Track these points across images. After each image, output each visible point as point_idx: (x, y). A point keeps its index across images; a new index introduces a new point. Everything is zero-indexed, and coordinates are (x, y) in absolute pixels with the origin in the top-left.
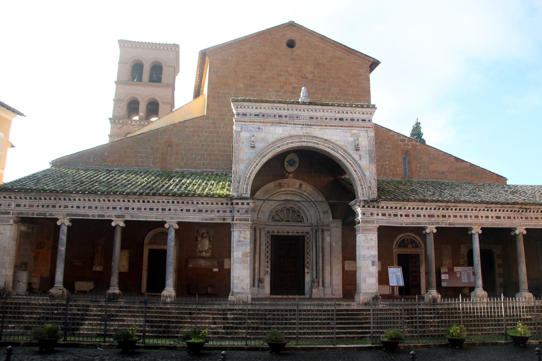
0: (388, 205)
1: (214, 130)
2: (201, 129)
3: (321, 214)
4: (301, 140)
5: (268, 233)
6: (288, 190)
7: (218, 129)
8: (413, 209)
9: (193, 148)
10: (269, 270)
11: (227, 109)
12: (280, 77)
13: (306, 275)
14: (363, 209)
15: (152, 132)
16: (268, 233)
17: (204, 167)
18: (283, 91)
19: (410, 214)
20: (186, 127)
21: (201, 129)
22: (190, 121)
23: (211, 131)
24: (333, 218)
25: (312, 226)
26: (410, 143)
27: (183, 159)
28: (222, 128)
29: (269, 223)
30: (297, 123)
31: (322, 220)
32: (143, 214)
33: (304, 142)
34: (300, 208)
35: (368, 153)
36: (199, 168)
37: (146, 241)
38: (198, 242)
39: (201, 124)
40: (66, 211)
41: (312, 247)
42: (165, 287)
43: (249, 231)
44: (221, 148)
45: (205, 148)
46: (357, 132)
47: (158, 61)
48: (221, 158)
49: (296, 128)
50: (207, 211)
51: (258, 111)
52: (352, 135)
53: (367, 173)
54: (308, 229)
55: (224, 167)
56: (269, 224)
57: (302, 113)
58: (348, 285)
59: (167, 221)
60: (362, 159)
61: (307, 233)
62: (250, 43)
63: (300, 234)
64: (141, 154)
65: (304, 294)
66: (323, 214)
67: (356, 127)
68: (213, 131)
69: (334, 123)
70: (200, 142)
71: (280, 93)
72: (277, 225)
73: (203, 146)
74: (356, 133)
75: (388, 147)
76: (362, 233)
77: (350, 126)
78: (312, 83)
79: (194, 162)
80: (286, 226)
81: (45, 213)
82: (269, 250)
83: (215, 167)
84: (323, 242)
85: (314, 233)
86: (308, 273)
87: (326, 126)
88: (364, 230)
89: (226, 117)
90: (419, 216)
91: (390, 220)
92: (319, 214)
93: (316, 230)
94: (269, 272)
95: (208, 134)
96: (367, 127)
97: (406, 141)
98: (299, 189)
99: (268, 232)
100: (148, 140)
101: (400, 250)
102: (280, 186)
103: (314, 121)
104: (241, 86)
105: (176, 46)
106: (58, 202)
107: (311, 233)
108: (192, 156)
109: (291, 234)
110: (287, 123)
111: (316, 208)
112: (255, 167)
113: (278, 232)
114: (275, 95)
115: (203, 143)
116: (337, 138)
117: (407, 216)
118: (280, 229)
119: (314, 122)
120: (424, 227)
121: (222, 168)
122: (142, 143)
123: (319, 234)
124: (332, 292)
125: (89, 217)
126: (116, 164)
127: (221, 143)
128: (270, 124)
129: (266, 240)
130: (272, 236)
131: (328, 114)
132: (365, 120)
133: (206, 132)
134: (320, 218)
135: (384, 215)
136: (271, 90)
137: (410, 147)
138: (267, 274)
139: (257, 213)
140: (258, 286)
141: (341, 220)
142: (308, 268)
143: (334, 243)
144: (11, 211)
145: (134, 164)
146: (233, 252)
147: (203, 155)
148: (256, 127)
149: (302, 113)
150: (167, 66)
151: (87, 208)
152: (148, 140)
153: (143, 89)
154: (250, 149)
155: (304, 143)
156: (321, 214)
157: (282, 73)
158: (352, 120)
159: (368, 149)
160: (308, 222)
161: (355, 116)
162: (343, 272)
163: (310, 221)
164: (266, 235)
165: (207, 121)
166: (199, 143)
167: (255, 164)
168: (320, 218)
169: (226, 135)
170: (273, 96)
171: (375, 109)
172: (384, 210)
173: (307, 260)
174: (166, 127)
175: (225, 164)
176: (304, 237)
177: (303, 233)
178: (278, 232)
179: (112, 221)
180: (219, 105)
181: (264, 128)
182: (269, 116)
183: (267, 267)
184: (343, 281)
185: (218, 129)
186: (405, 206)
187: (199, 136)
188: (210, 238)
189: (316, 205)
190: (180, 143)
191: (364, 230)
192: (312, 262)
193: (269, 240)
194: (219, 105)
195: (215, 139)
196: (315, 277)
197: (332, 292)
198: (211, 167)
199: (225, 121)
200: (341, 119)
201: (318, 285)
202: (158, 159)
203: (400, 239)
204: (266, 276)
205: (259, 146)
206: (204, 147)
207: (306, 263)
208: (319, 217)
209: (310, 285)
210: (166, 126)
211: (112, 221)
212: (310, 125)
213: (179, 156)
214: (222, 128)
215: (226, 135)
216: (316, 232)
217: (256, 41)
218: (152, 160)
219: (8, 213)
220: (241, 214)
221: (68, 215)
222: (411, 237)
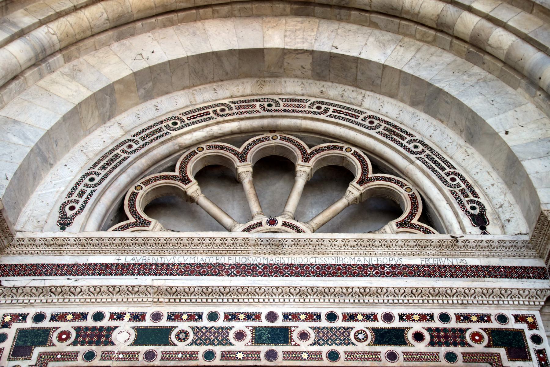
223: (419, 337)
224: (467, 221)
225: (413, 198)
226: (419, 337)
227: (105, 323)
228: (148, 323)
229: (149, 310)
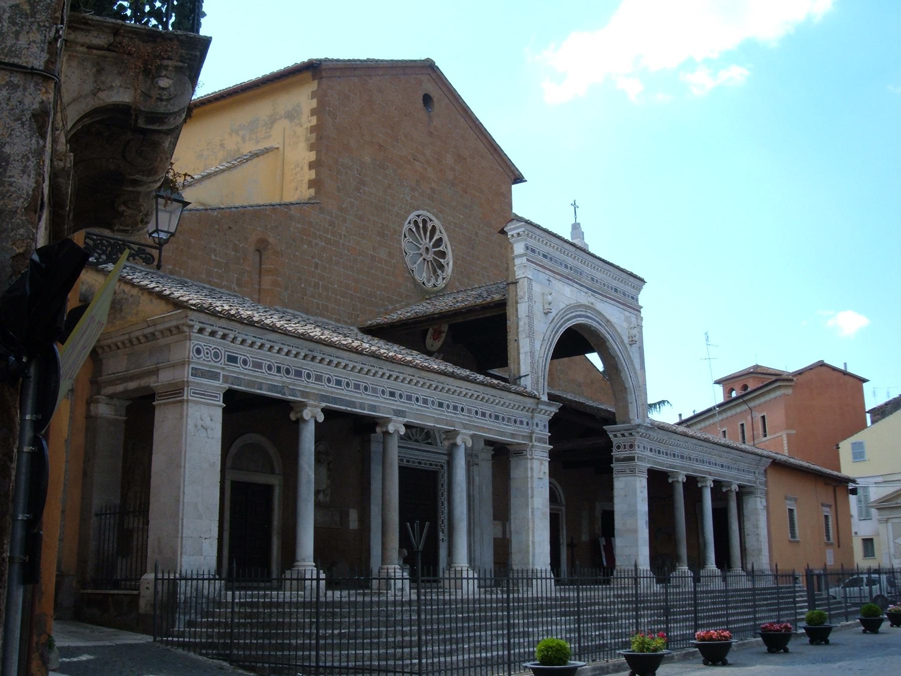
1: (332, 238)
2: (312, 230)
7: (338, 237)
9: (301, 266)
11: (349, 200)
12: (417, 163)
17: (318, 311)
28: (343, 237)
32: (432, 413)
39: (314, 219)
40: (319, 387)
44: (342, 279)
45: (319, 271)
48: (342, 299)
52: (627, 320)
62: (379, 77)
64: (215, 255)
68: (330, 239)
70: (312, 258)
76: (639, 476)
78: (453, 188)
79: (303, 298)
81: (283, 387)
83: (334, 316)
89: (348, 217)
95: (323, 244)
100: (230, 228)
104: (368, 159)
106: (307, 364)
113: (408, 461)
115: (316, 260)
120: (673, 472)
121: (344, 321)
125: (355, 408)
126: (170, 267)
127: (343, 268)
128: (558, 277)
136: (405, 184)
144: (222, 373)
145: (204, 276)
146: (532, 497)
147: (316, 286)
151: (352, 388)
152: (230, 228)
154: (543, 314)
157: (419, 155)
166: (310, 258)
169: (349, 254)
179: (388, 420)
180: (338, 187)
181: (553, 282)
188: (329, 464)
194: (338, 187)
195: (334, 258)
198: (329, 314)
199: (347, 225)
206: (317, 270)
211: (388, 420)
213: (279, 279)
214: (343, 237)
218: (236, 276)
219: (214, 376)
221: (323, 398)
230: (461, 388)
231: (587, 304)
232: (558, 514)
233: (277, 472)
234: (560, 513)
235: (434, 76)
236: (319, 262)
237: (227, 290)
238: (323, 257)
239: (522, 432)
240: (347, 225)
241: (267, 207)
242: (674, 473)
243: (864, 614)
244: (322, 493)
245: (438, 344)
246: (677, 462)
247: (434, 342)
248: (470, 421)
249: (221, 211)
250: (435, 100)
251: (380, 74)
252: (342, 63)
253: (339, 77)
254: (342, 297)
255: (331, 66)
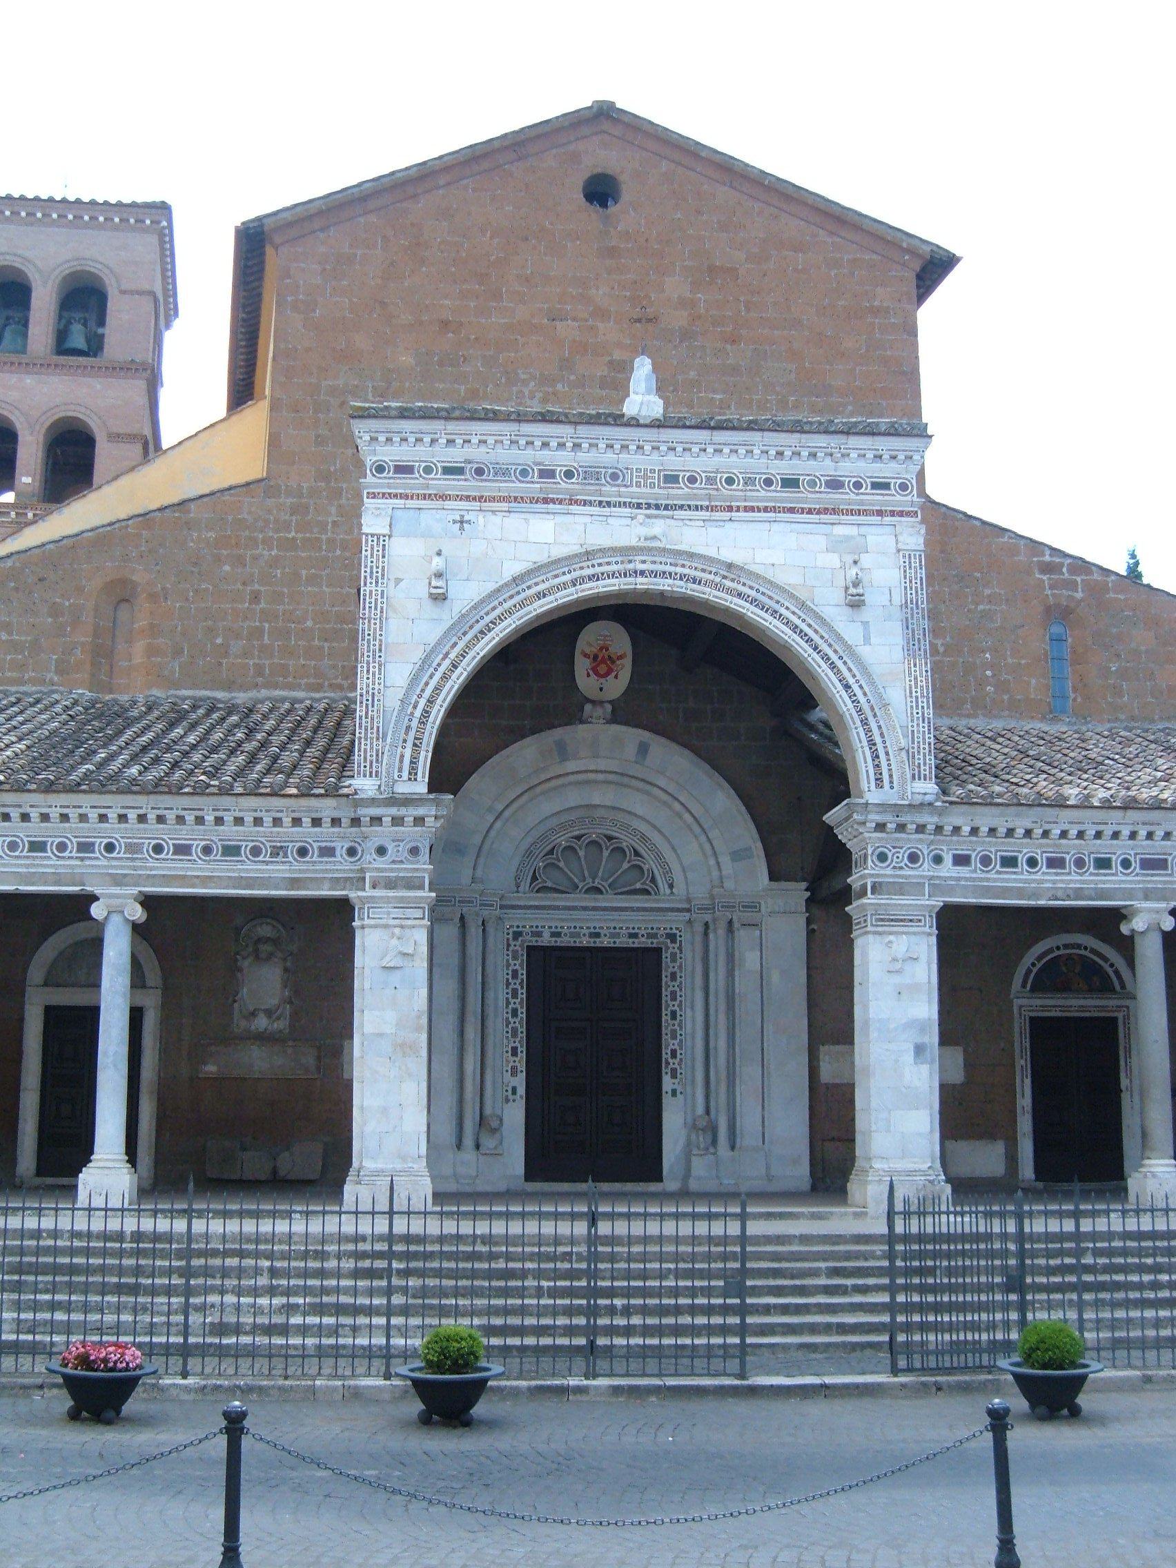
0: (976, 823)
1: (300, 535)
2: (247, 533)
3: (725, 860)
4: (631, 566)
5: (515, 939)
6: (592, 767)
8: (1080, 835)
10: (520, 1082)
12: (558, 324)
13: (667, 1100)
14: (880, 839)
15: (52, 546)
16: (515, 939)
18: (572, 377)
19: (1068, 857)
20: (189, 525)
21: (247, 533)
22: (205, 500)
23: (288, 539)
24: (773, 877)
25: (689, 910)
26: (1079, 579)
27: (178, 652)
29: (519, 899)
30: (613, 499)
31: (729, 884)
33: (642, 573)
34: (644, 838)
35: (898, 614)
36: (243, 688)
37: (36, 973)
38: (239, 975)
39: (249, 513)
41: (689, 992)
42: (92, 1153)
43: (421, 926)
44: (327, 607)
45: (263, 605)
46: (853, 531)
47: (89, 272)
48: (326, 645)
49: (611, 520)
50: (256, 851)
51: (456, 455)
52: (834, 546)
53: (896, 696)
54: (675, 922)
55: (339, 681)
56: (521, 903)
57: (631, 460)
58: (833, 1139)
59: (98, 891)
60: (873, 640)
61: (672, 937)
63: (643, 939)
64: (10, 634)
65: (658, 1178)
66: (733, 860)
67: (851, 512)
68: (294, 539)
69: (761, 495)
70: (244, 584)
71: (559, 386)
72: (550, 908)
73: (256, 597)
74: (852, 537)
75: (989, 596)
77: (826, 511)
79: (220, 664)
80: (585, 908)
82: (521, 1003)
83: (304, 681)
84: (730, 974)
85: (699, 938)
86: (674, 1093)
87: (730, 509)
88: (882, 920)
89: (344, 486)
90: (1103, 864)
91: (988, 880)
92: (718, 863)
93: (706, 924)
94: (521, 1091)
96: (893, 513)
97: (1064, 570)
98: (636, 762)
99: (514, 933)
101: (1039, 1002)
102: (563, 752)
103: (680, 492)
104: (407, 359)
105: (163, 208)
107: (685, 937)
108: (215, 637)
109: (605, 942)
110: (572, 502)
111: (703, 838)
112: (445, 677)
113: (554, 935)
114: (539, 395)
115: (257, 587)
116: (777, 557)
117: (1055, 863)
118: (563, 920)
119: (681, 491)
120: (1126, 907)
122: (17, 589)
123: (718, 939)
124: (768, 1167)
128: (504, 506)
129: (508, 965)
130: (531, 949)
131: (735, 463)
132: (886, 486)
133: (267, 542)
134: (721, 878)
135: (961, 860)
136: (523, 376)
137: (1079, 595)
138: (511, 1097)
139: (469, 860)
140: (478, 1147)
141: (804, 885)
142: (674, 1076)
143: (775, 977)
147: (258, 633)
148: (451, 518)
149: (631, 460)
150: (123, 292)
153: (29, 380)
155: (640, 580)
156: (725, 860)
158: (835, 484)
159: (898, 599)
160: (672, 893)
161: (849, 469)
162: (812, 1089)
163: (680, 889)
164: (509, 945)
165: (271, 502)
167: (447, 662)
168: (721, 878)
169: (347, 554)
170: (532, 398)
171: (926, 440)
172: (965, 842)
173: (668, 1044)
174: (109, 528)
175: (343, 667)
176: (657, 951)
177: (654, 936)
178: (554, 935)
180: (318, 436)
182: (502, 472)
183: (514, 1072)
184: (811, 1127)
185: (315, 530)
186: (1047, 827)
187: (240, 561)
189: (705, 827)
190: (163, 589)
191: (882, 920)
192: (689, 1052)
193: (521, 965)
195: (304, 572)
196: (700, 1110)
197: (768, 1167)
199: (343, 501)
200: (790, 483)
201: (714, 1142)
202: (78, 652)
203: (1039, 958)
204: (505, 1106)
205: (465, 594)
206: (258, 603)
207: (666, 1053)
208: (715, 873)
209: (682, 1142)
210: (110, 524)
212: (666, 508)
213: (161, 640)
215: (347, 554)
216: (706, 934)
217: (465, 182)
220: (394, 862)
222: (1082, 952)
223: (643, 936)
224: (666, 886)
225: (648, 870)
226: (643, 936)
227: (540, 929)
228: (553, 930)
229: (553, 925)
230: (80, 807)
231: (634, 542)
232: (1114, 1020)
233: (149, 983)
234: (1120, 1016)
235: (618, 131)
236: (262, 589)
237: (34, 685)
238: (275, 576)
239: (326, 871)
240: (343, 501)
241: (130, 522)
242: (1129, 908)
243: (1028, 1358)
244: (262, 1015)
245: (617, 685)
246: (1134, 879)
247: (603, 680)
248: (135, 868)
249: (23, 555)
250: (623, 178)
251: (442, 182)
252: (321, 202)
253: (322, 230)
254: (326, 640)
255: (290, 218)
